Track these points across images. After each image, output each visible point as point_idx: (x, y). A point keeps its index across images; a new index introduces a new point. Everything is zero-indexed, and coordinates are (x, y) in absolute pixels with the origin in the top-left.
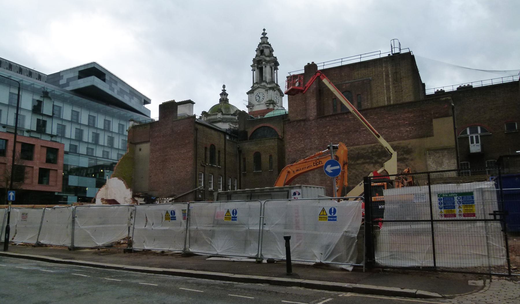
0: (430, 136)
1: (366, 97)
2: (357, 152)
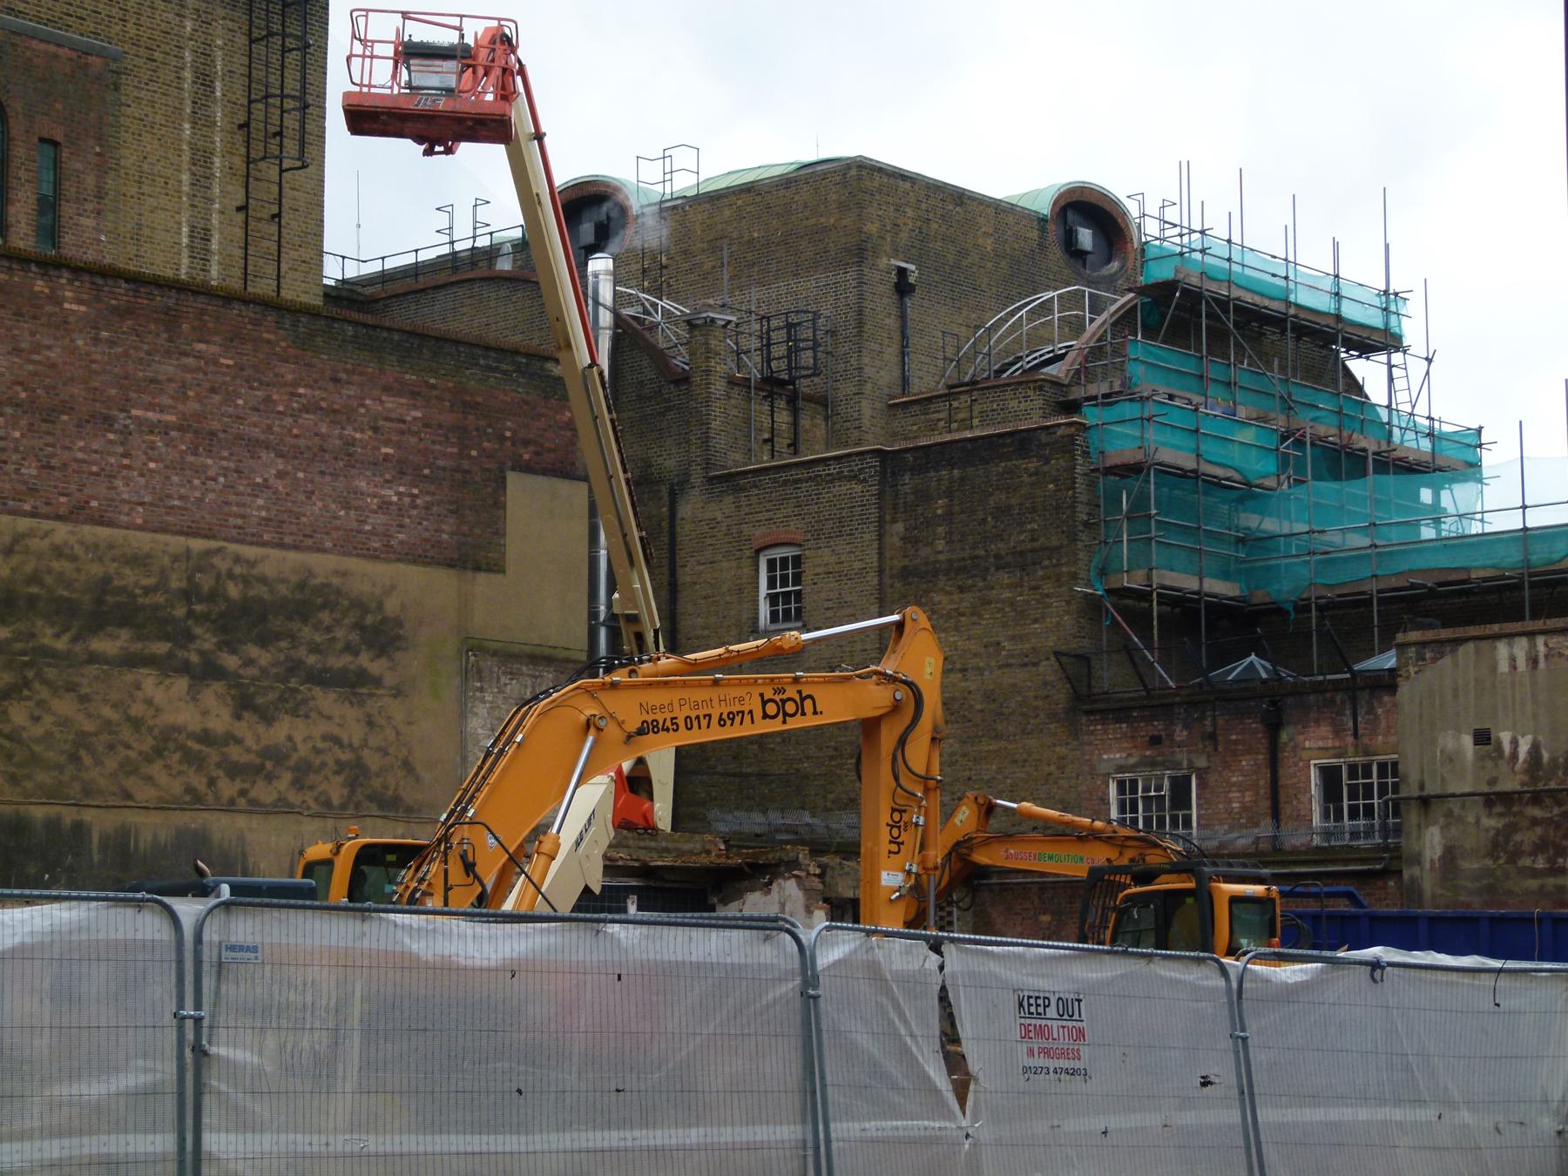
0: (490, 570)
1: (90, 181)
2: (96, 570)
